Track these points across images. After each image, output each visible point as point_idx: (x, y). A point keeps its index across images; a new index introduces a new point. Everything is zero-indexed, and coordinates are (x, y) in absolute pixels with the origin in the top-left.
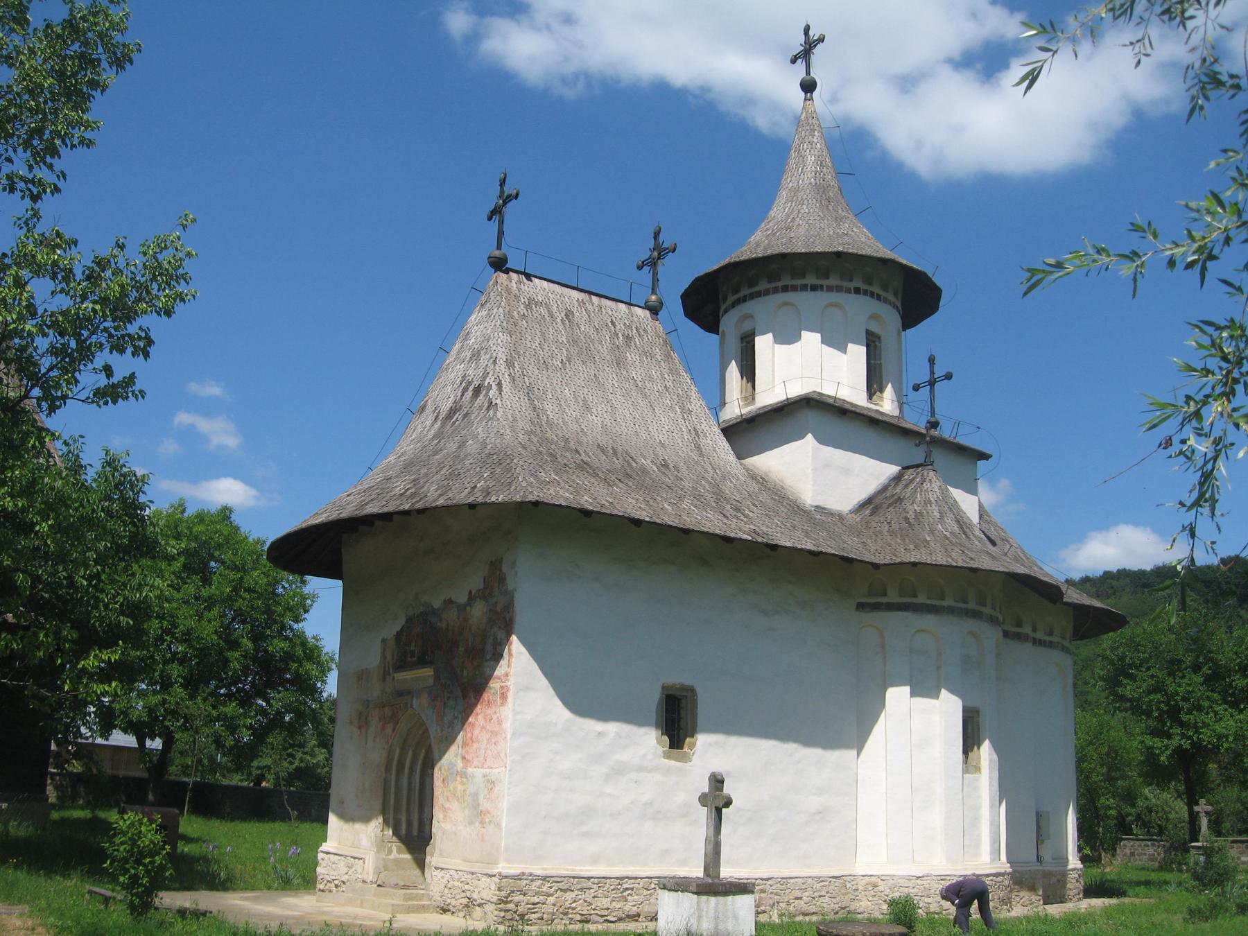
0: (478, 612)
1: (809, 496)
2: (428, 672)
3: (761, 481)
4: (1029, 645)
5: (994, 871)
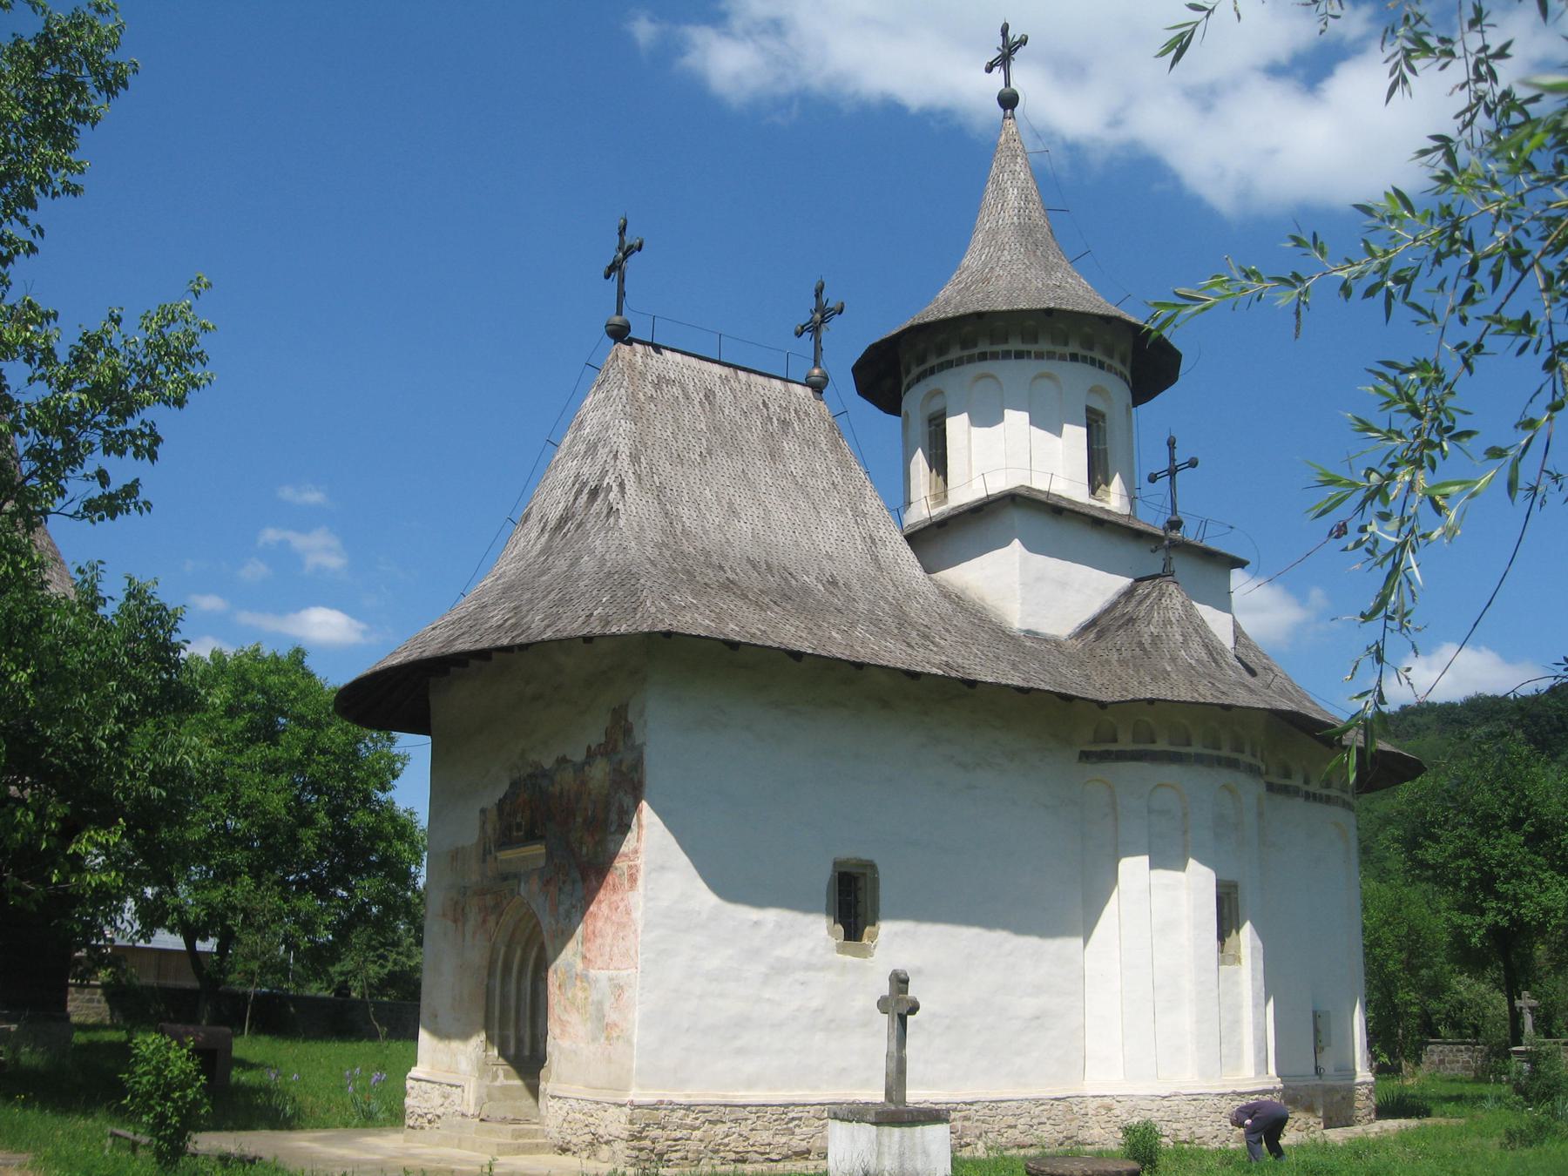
0: (599, 772)
1: (1017, 617)
2: (538, 849)
3: (956, 600)
4: (1300, 801)
5: (1260, 1087)
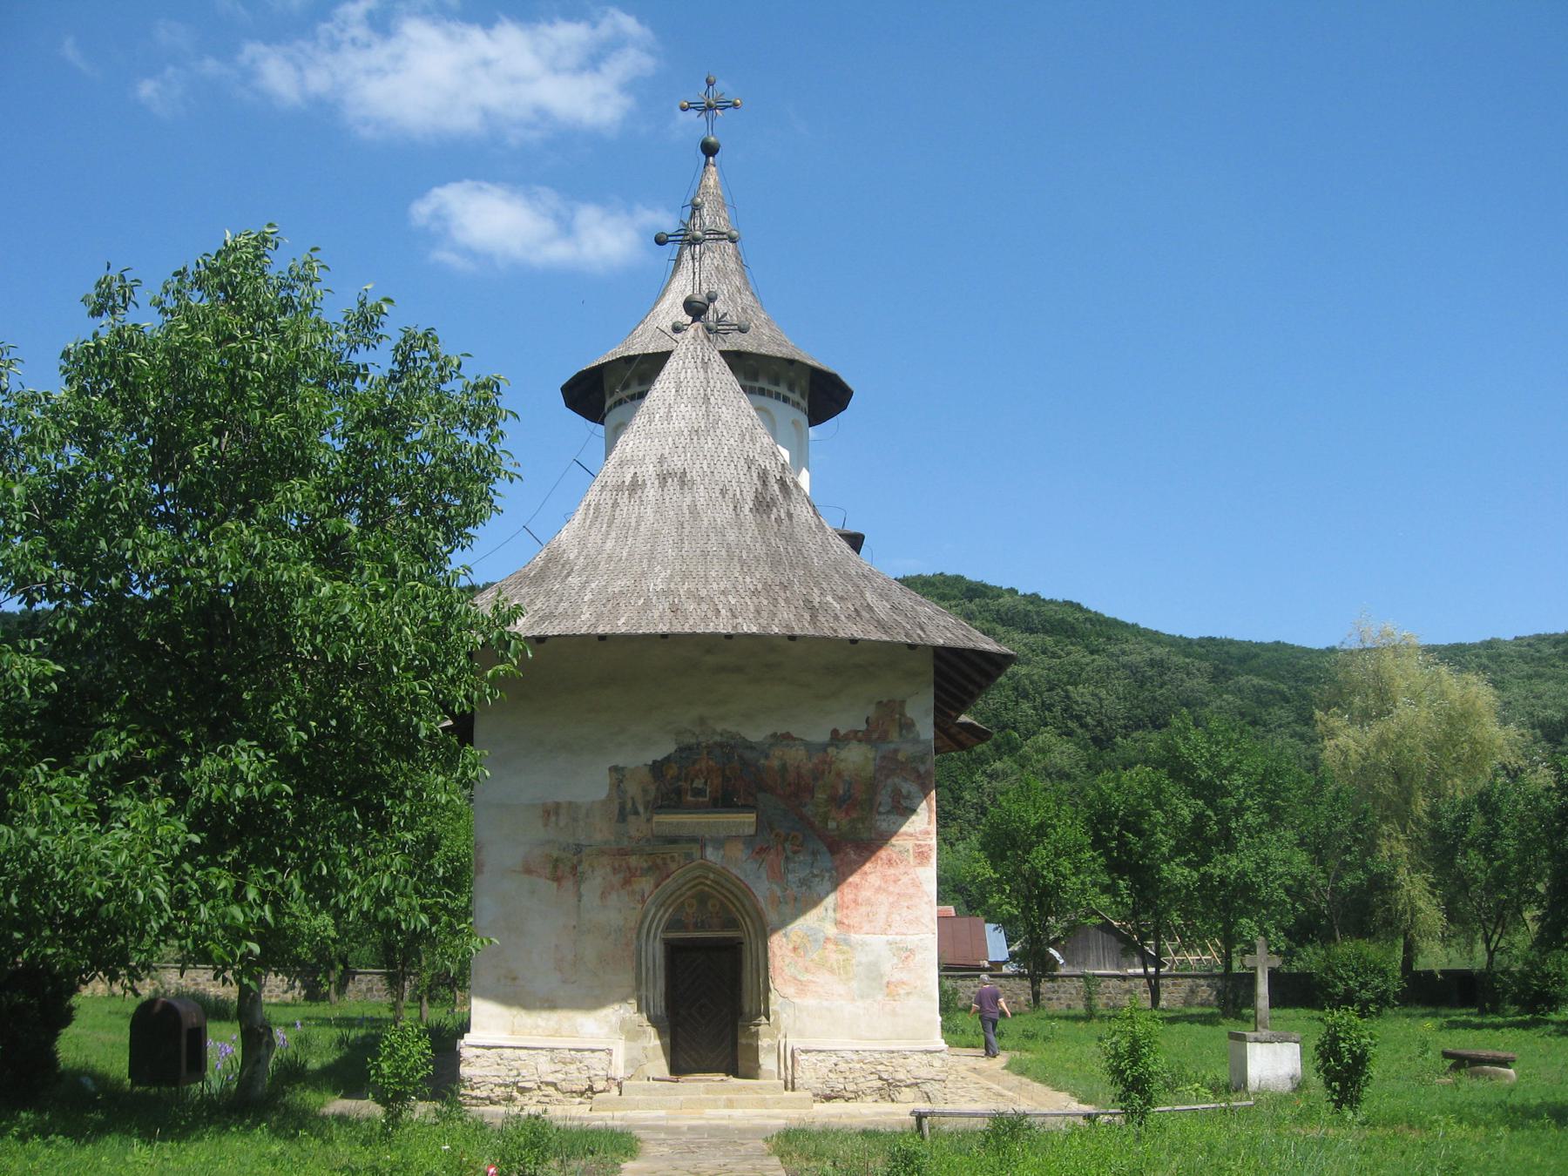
2: (751, 818)
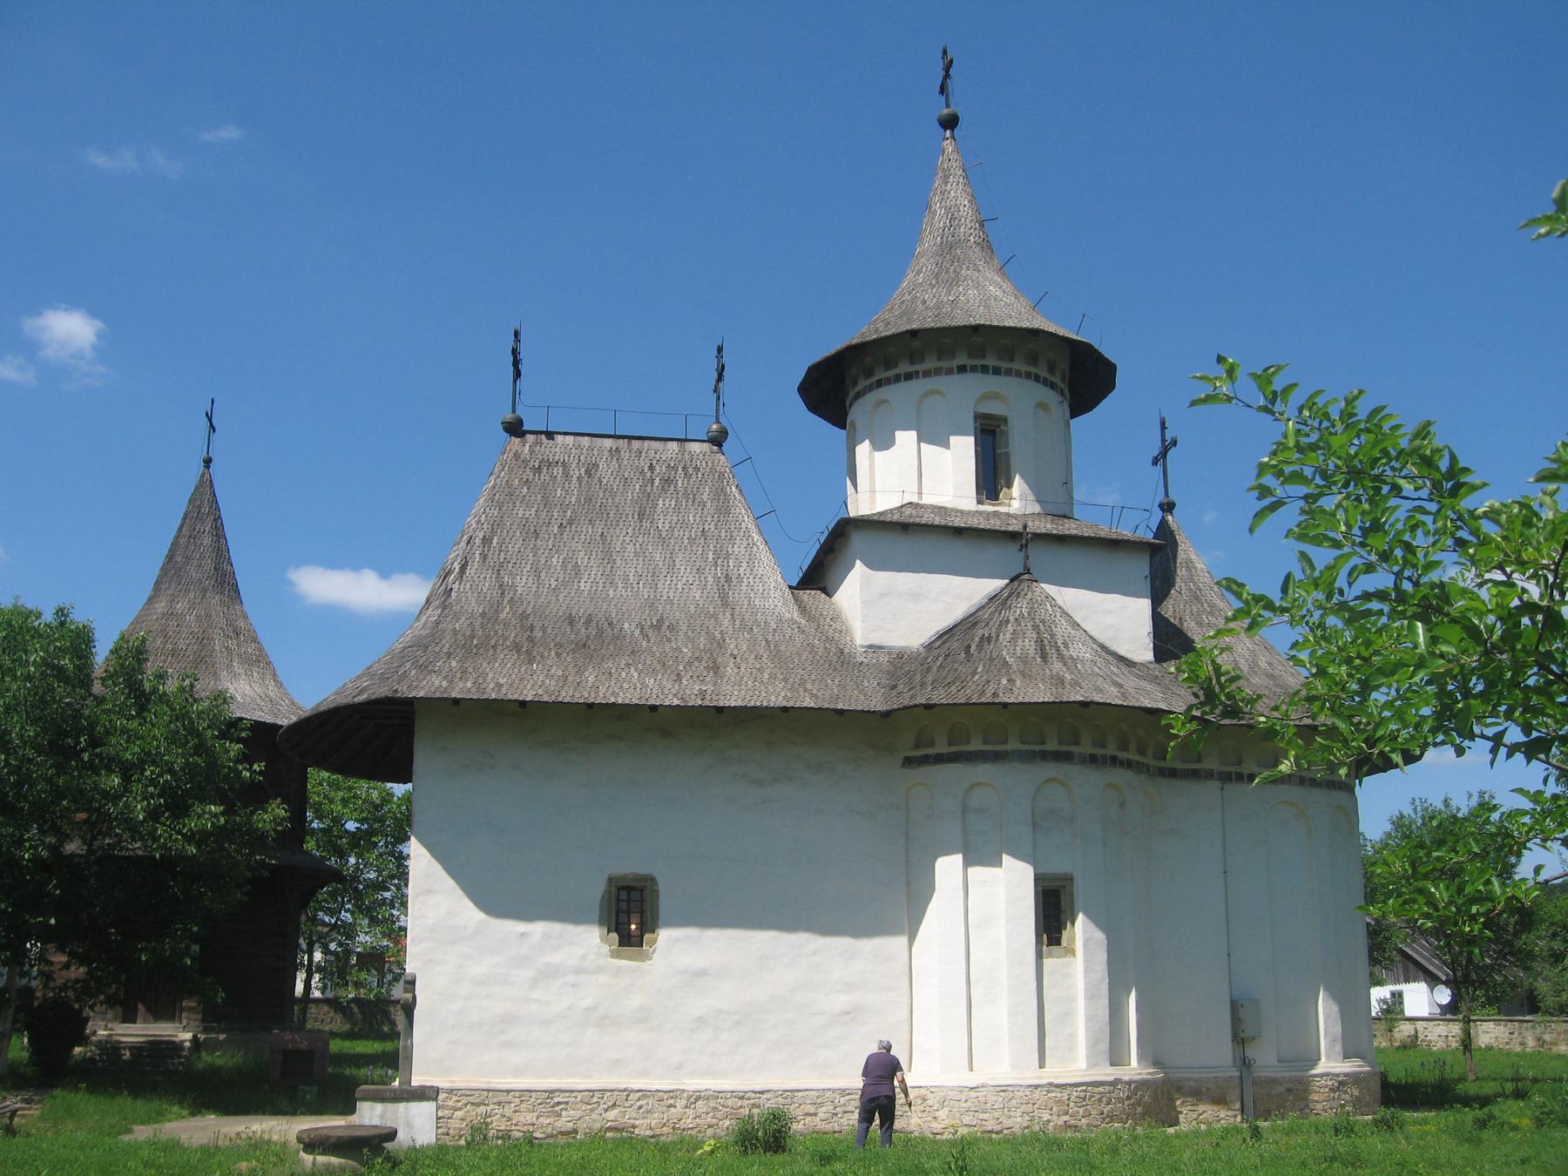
4: (1213, 786)
